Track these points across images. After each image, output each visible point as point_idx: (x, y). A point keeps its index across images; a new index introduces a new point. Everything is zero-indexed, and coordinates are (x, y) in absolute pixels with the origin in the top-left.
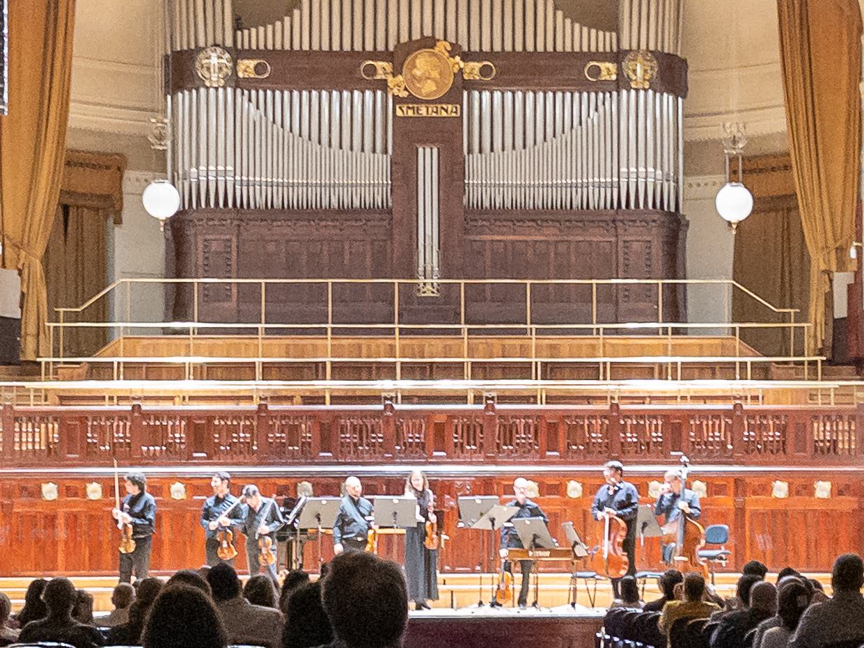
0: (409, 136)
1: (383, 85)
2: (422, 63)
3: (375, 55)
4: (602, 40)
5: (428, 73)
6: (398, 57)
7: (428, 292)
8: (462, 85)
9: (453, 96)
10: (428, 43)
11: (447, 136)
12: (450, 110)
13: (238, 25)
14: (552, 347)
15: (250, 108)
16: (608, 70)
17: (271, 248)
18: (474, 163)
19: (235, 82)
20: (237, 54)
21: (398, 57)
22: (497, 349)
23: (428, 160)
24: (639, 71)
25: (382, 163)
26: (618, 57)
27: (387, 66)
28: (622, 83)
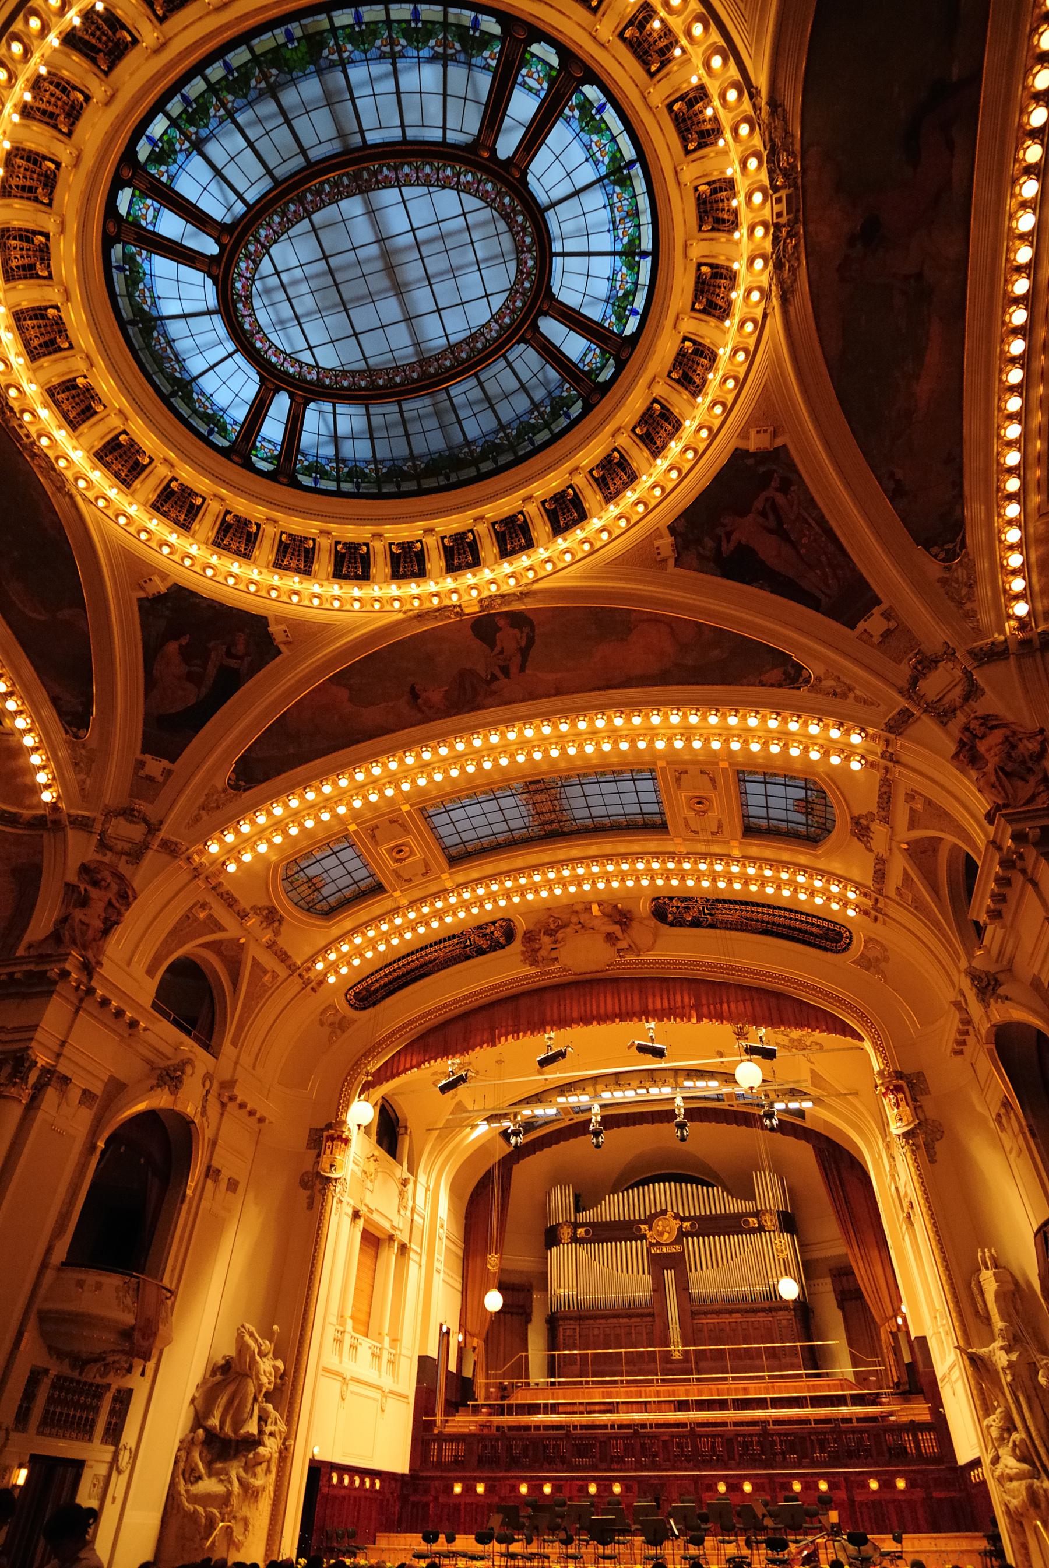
0: (659, 1263)
1: (643, 1237)
2: (659, 1224)
3: (641, 1222)
4: (748, 1206)
5: (666, 1230)
6: (649, 1221)
7: (677, 1356)
8: (682, 1234)
9: (678, 1241)
10: (664, 1212)
11: (676, 1262)
12: (677, 1249)
13: (578, 1210)
14: (745, 1389)
15: (583, 1252)
16: (753, 1221)
17: (596, 1332)
18: (692, 1276)
19: (575, 1240)
20: (576, 1226)
21: (649, 1221)
22: (715, 1392)
23: (669, 1276)
24: (769, 1222)
25: (647, 1279)
26: (756, 1214)
27: (646, 1227)
28: (761, 1229)
